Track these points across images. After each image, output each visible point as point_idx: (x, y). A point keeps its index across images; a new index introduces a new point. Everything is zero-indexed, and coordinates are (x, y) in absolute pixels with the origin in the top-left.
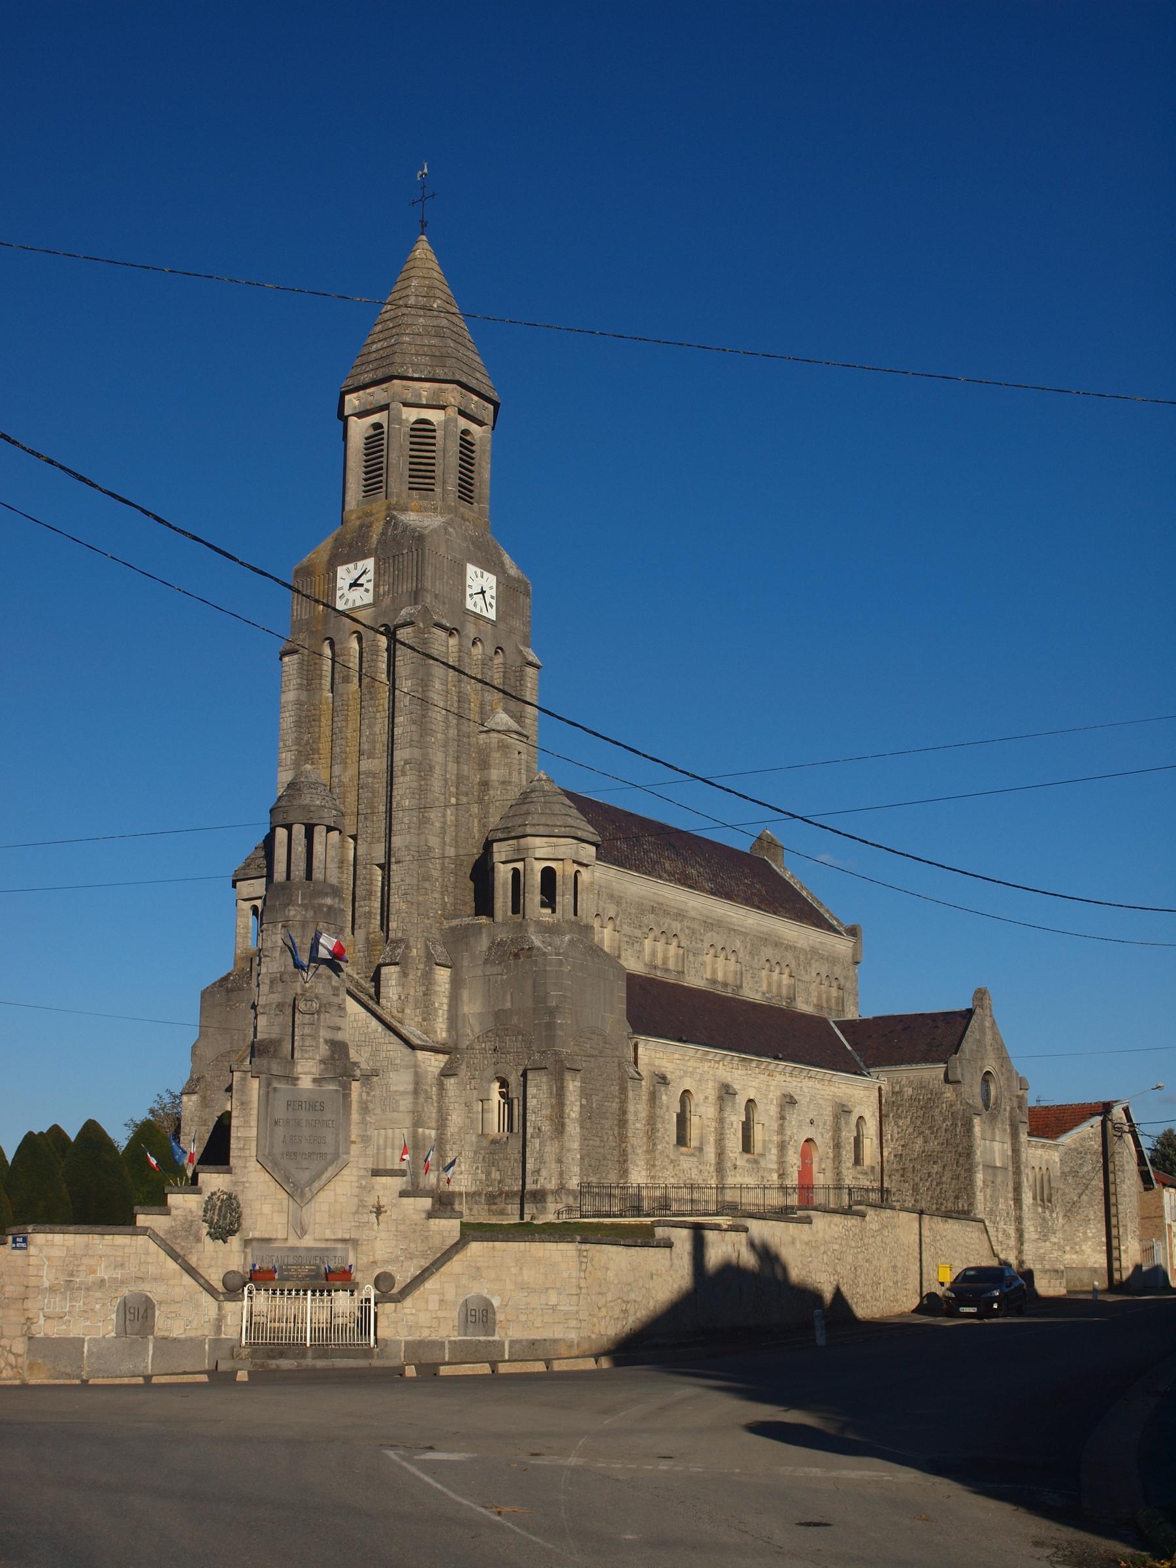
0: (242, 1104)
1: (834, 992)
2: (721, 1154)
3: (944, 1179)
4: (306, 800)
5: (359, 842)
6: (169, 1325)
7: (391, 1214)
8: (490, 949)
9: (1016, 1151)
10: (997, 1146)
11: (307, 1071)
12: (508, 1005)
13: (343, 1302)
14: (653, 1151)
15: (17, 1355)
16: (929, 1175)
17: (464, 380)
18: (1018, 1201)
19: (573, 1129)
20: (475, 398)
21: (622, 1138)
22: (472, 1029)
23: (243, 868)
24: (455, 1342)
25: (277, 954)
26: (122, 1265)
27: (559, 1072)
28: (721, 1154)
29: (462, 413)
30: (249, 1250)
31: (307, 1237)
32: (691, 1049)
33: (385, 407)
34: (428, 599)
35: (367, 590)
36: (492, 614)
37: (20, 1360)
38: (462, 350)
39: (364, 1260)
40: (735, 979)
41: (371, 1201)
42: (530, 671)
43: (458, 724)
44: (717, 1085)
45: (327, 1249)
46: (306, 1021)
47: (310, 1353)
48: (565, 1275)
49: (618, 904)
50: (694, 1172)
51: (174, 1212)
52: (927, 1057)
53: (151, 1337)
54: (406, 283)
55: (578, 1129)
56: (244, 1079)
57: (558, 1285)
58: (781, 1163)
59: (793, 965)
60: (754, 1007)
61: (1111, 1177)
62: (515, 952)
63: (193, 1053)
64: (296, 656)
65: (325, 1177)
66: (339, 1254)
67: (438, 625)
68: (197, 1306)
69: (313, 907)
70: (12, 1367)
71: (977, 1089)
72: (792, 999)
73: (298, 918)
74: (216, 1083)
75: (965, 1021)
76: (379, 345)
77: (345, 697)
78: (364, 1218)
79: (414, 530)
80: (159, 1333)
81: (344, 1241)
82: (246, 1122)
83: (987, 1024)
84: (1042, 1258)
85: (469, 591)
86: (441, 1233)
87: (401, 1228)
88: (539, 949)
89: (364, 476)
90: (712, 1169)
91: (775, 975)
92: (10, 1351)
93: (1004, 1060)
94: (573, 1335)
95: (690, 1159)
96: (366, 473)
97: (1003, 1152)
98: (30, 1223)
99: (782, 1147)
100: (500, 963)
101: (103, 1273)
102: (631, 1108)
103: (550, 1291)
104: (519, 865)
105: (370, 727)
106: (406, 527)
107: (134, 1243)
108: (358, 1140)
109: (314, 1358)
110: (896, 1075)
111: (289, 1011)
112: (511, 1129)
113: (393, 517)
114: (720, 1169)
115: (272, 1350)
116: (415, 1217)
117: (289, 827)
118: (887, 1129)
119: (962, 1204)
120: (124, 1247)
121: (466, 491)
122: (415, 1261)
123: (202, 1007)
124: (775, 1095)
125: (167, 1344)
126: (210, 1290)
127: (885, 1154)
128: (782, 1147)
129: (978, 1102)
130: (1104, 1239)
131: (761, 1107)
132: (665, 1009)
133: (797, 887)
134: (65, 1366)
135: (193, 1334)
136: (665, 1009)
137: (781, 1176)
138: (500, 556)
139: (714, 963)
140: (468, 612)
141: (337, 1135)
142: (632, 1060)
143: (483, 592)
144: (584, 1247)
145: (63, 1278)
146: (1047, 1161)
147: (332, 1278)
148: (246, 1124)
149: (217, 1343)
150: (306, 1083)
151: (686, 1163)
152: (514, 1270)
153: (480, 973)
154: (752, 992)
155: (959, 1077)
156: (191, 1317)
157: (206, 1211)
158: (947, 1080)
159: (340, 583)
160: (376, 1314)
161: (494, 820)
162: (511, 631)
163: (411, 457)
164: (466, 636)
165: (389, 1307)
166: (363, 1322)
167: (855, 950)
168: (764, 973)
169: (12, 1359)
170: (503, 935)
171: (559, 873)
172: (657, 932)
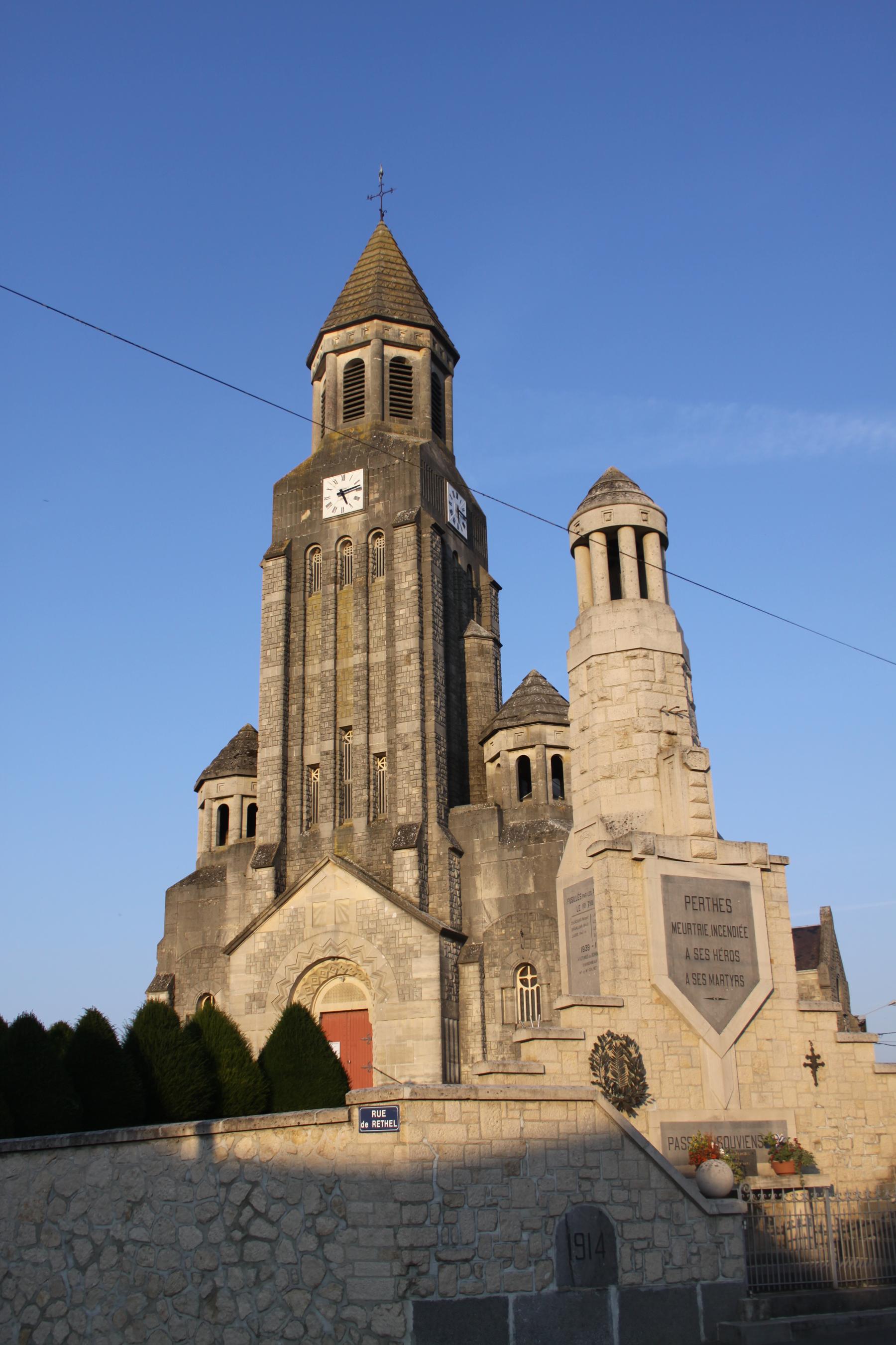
80: (627, 1278)
123: (166, 906)
135: (674, 1277)
159: (326, 493)
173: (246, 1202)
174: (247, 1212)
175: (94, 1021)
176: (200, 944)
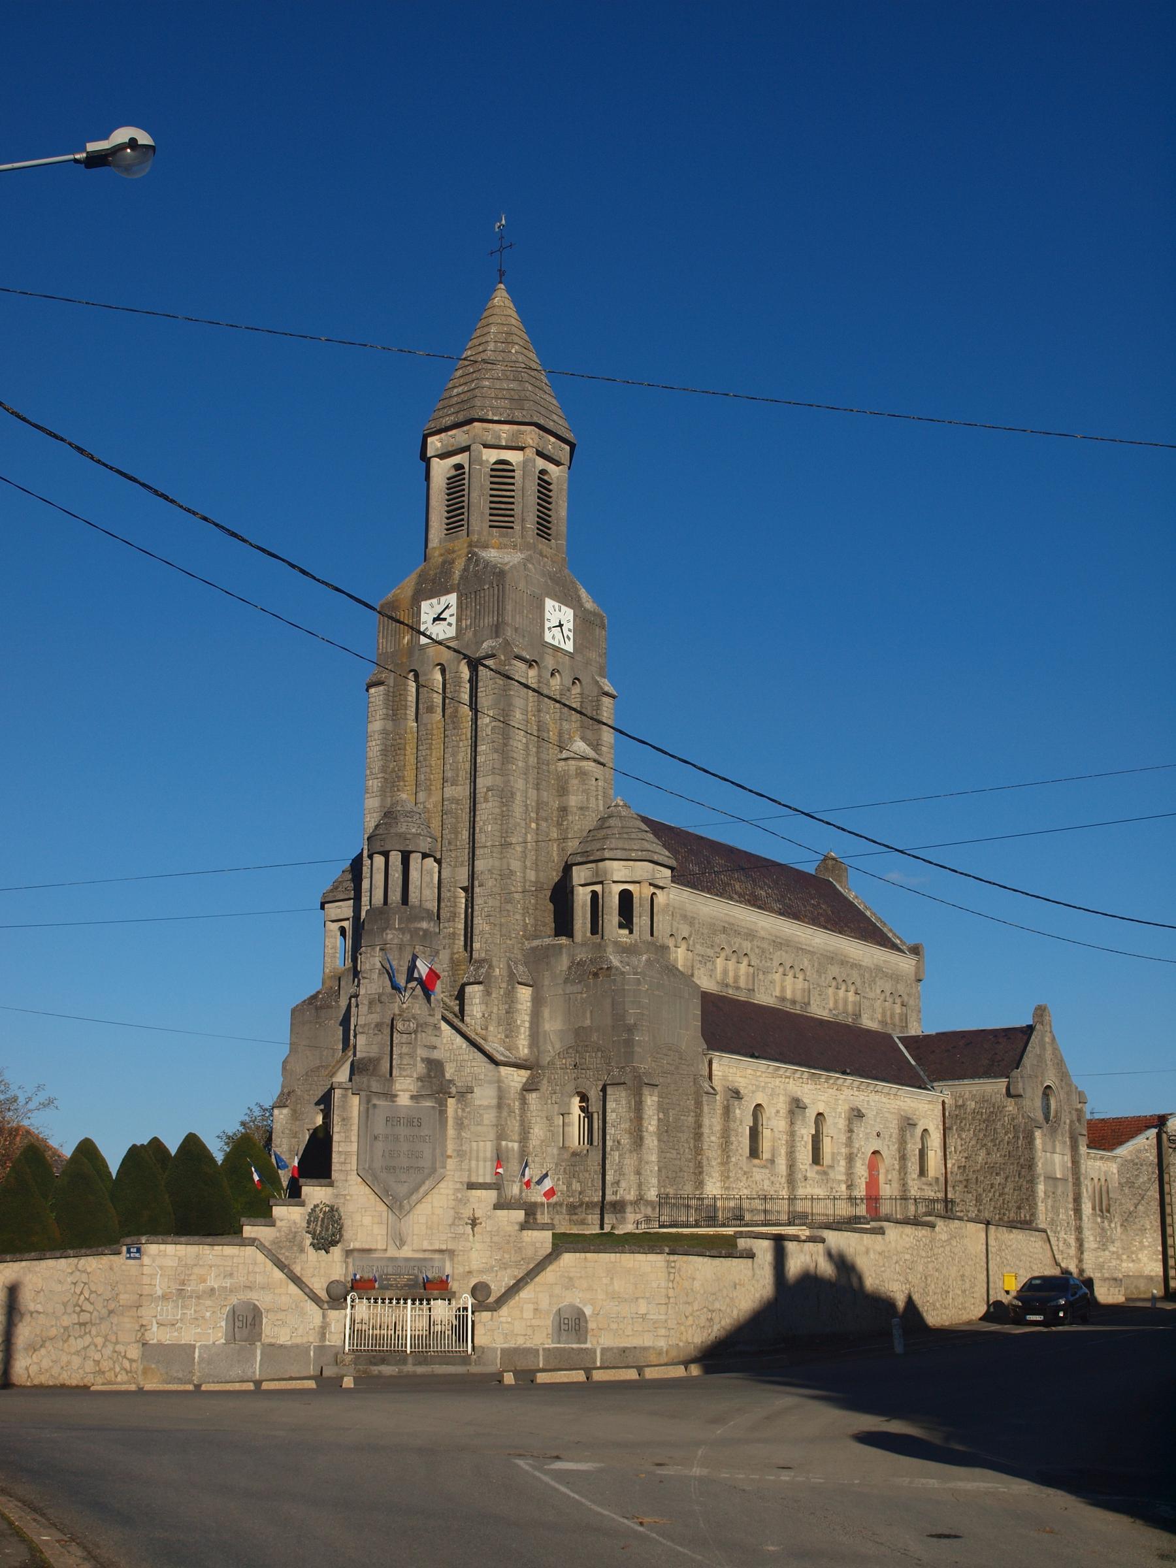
0: (343, 1120)
1: (898, 1009)
2: (791, 1166)
3: (1006, 1190)
4: (402, 828)
5: (443, 865)
6: (276, 1332)
7: (486, 1225)
8: (570, 968)
9: (1075, 1163)
10: (1057, 1158)
11: (405, 1088)
12: (588, 1022)
13: (441, 1310)
14: (727, 1163)
15: (131, 1361)
16: (992, 1186)
17: (542, 422)
18: (1078, 1211)
19: (651, 1142)
20: (553, 439)
21: (698, 1151)
22: (553, 1046)
23: (331, 891)
24: (549, 1349)
25: (375, 976)
26: (231, 1274)
27: (638, 1086)
28: (791, 1166)
29: (540, 454)
30: (350, 1260)
31: (405, 1248)
32: (763, 1067)
33: (466, 449)
34: (509, 633)
35: (450, 624)
36: (569, 647)
37: (134, 1365)
38: (540, 393)
39: (460, 1270)
40: (803, 997)
41: (467, 1213)
42: (606, 701)
43: (538, 752)
44: (788, 1099)
45: (425, 1259)
46: (404, 1041)
47: (410, 1360)
48: (654, 1285)
49: (691, 924)
50: (767, 1183)
51: (278, 1223)
52: (989, 1072)
53: (258, 1344)
54: (486, 330)
55: (656, 1142)
56: (345, 1096)
57: (647, 1295)
58: (850, 1174)
59: (858, 983)
60: (821, 1023)
61: (1167, 1187)
62: (594, 972)
63: (284, 1068)
64: (382, 688)
65: (422, 1190)
66: (436, 1264)
68: (303, 1313)
69: (410, 931)
70: (127, 1372)
71: (1038, 1103)
72: (858, 1015)
73: (396, 941)
74: (306, 1097)
75: (1025, 1038)
76: (460, 389)
77: (429, 727)
78: (460, 1230)
79: (495, 566)
80: (266, 1340)
81: (441, 1251)
82: (347, 1137)
83: (1047, 1040)
84: (1101, 1267)
85: (547, 624)
86: (533, 1244)
87: (495, 1239)
88: (617, 968)
89: (446, 515)
90: (783, 1180)
91: (841, 993)
92: (125, 1357)
93: (1064, 1076)
94: (662, 1343)
95: (763, 1170)
96: (448, 512)
97: (1063, 1165)
98: (143, 1234)
99: (850, 1159)
100: (580, 982)
101: (213, 1282)
102: (706, 1122)
103: (641, 1301)
104: (598, 888)
105: (454, 755)
106: (487, 564)
107: (242, 1254)
108: (455, 1154)
109: (414, 1365)
110: (959, 1089)
111: (387, 1031)
112: (591, 1142)
113: (475, 554)
114: (791, 1180)
115: (374, 1357)
116: (509, 1229)
117: (386, 854)
118: (952, 1141)
119: (1024, 1214)
120: (233, 1257)
121: (544, 528)
122: (509, 1271)
123: (292, 1024)
124: (843, 1108)
125: (273, 1350)
126: (315, 1299)
127: (949, 1165)
128: (850, 1159)
129: (1039, 1115)
130: (1160, 1248)
131: (829, 1121)
132: (738, 1026)
133: (861, 907)
134: (177, 1371)
135: (298, 1341)
136: (738, 1026)
137: (850, 1187)
138: (577, 590)
139: (783, 981)
140: (546, 645)
141: (434, 1149)
142: (707, 1074)
143: (561, 625)
144: (672, 1258)
145: (175, 1287)
146: (1105, 1172)
147: (428, 1287)
148: (347, 1139)
149: (321, 1349)
150: (404, 1100)
151: (759, 1175)
152: (605, 1281)
153: (561, 992)
154: (820, 1009)
155: (1021, 1092)
156: (298, 1326)
157: (309, 1222)
158: (1009, 1094)
159: (423, 617)
160: (473, 1322)
161: (573, 845)
162: (588, 663)
163: (492, 496)
164: (546, 667)
165: (486, 1315)
166: (460, 1328)
167: (917, 968)
168: (831, 991)
169: (127, 1364)
170: (582, 955)
171: (636, 895)
172: (728, 951)
173: (82, 1293)
174: (82, 1297)
175: (192, 1143)
176: (318, 1063)
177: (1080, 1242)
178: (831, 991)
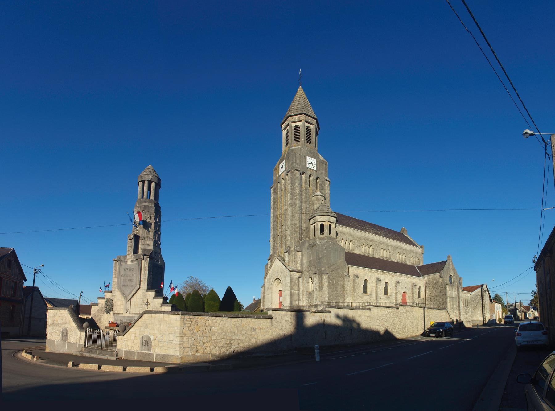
1: (417, 260)
9: (458, 294)
10: (453, 292)
18: (459, 305)
42: (327, 182)
49: (353, 237)
52: (436, 272)
60: (394, 263)
67: (296, 170)
71: (448, 279)
93: (455, 273)
119: (444, 306)
129: (448, 282)
132: (354, 259)
136: (354, 259)
140: (307, 168)
168: (398, 255)
172: (365, 244)
177: (460, 313)
178: (398, 255)
